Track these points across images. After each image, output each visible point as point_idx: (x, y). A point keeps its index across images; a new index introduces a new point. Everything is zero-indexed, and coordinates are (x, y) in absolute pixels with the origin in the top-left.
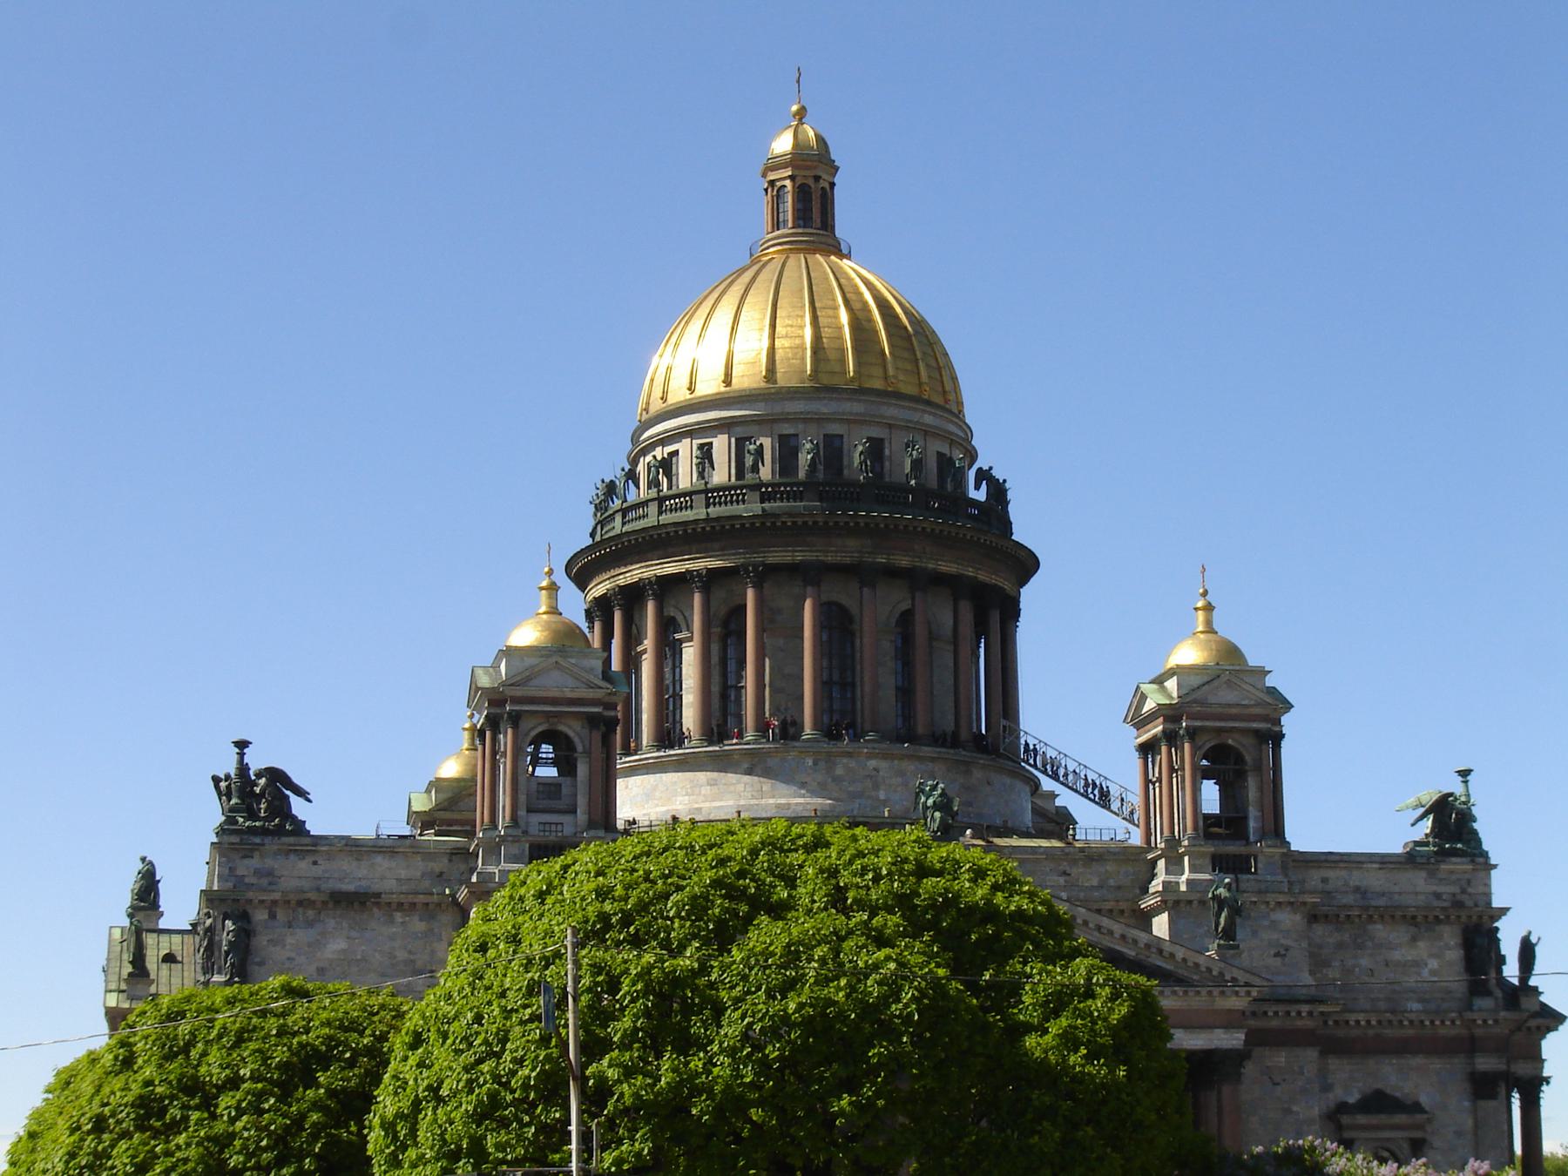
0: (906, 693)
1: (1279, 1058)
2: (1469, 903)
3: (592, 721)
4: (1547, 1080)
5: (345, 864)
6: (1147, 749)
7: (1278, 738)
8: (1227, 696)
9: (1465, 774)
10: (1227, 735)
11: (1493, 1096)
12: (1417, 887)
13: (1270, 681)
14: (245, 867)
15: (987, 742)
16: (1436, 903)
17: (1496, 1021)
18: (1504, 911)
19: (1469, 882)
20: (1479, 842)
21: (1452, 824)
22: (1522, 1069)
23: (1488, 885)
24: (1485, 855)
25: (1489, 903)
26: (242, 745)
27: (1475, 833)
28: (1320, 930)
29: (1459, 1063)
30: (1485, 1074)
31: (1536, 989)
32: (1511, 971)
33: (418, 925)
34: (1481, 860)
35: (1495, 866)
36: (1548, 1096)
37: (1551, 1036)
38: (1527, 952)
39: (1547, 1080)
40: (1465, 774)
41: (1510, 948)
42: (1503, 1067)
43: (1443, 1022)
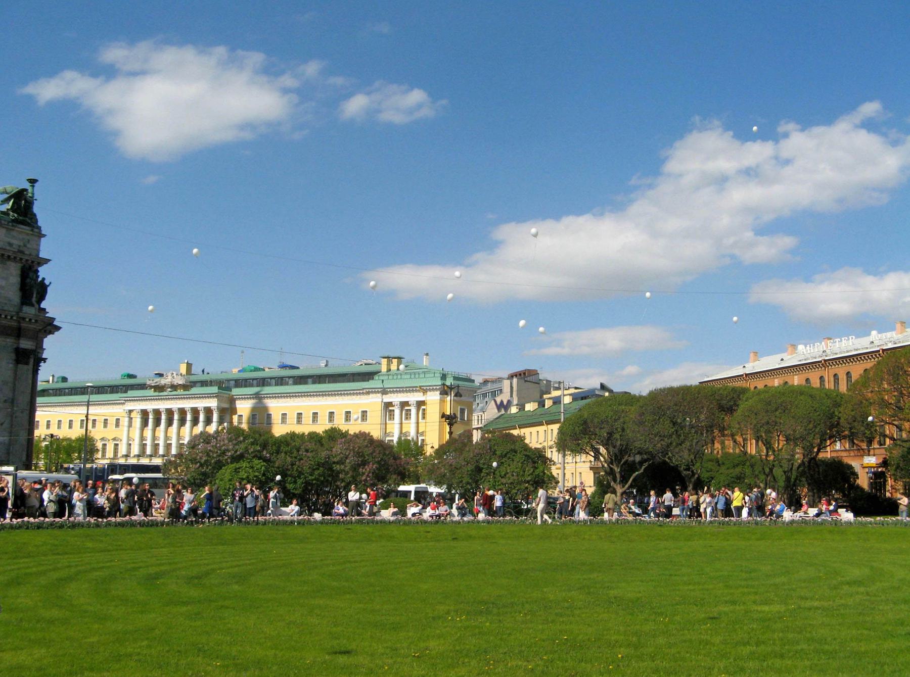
2: (27, 252)
4: (45, 360)
9: (33, 182)
11: (27, 363)
16: (8, 248)
17: (36, 321)
18: (47, 261)
19: (29, 241)
20: (37, 221)
23: (39, 245)
24: (39, 228)
25: (38, 255)
27: (35, 215)
29: (10, 341)
30: (25, 350)
31: (44, 309)
34: (36, 230)
35: (44, 236)
37: (50, 337)
39: (45, 360)
40: (33, 182)
42: (34, 348)
43: (6, 317)
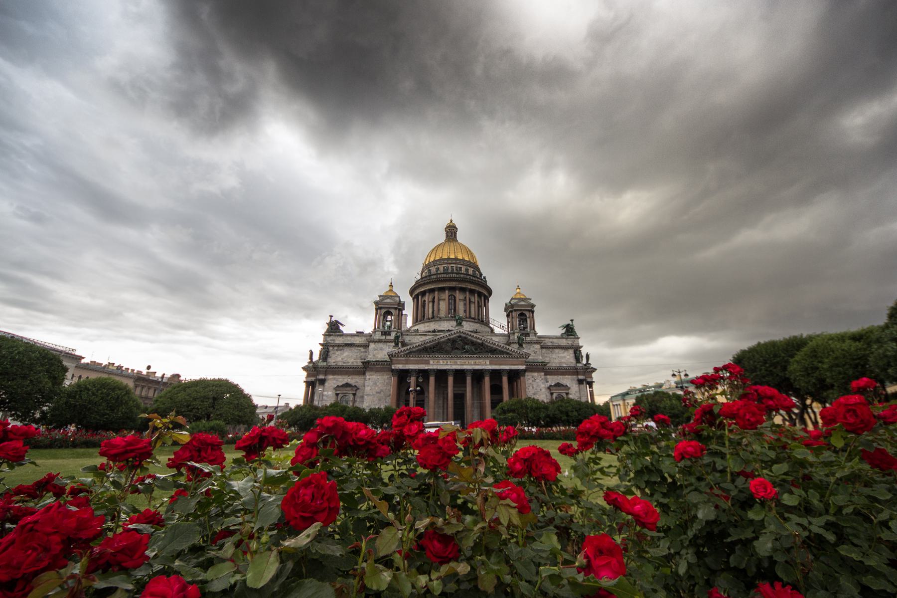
0: (465, 311)
1: (536, 374)
3: (396, 308)
5: (349, 338)
6: (508, 316)
7: (533, 312)
8: (523, 303)
9: (572, 321)
10: (522, 313)
12: (564, 342)
13: (532, 302)
14: (329, 339)
15: (484, 321)
21: (569, 330)
22: (589, 380)
26: (331, 316)
28: (544, 350)
29: (575, 377)
32: (584, 362)
33: (362, 349)
36: (594, 385)
38: (588, 356)
40: (572, 321)
41: (584, 354)
